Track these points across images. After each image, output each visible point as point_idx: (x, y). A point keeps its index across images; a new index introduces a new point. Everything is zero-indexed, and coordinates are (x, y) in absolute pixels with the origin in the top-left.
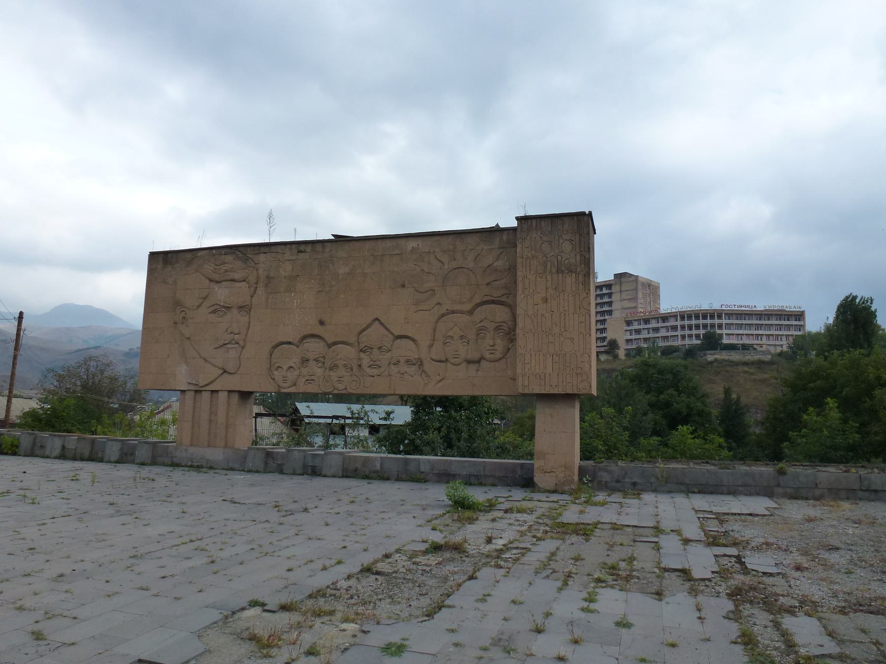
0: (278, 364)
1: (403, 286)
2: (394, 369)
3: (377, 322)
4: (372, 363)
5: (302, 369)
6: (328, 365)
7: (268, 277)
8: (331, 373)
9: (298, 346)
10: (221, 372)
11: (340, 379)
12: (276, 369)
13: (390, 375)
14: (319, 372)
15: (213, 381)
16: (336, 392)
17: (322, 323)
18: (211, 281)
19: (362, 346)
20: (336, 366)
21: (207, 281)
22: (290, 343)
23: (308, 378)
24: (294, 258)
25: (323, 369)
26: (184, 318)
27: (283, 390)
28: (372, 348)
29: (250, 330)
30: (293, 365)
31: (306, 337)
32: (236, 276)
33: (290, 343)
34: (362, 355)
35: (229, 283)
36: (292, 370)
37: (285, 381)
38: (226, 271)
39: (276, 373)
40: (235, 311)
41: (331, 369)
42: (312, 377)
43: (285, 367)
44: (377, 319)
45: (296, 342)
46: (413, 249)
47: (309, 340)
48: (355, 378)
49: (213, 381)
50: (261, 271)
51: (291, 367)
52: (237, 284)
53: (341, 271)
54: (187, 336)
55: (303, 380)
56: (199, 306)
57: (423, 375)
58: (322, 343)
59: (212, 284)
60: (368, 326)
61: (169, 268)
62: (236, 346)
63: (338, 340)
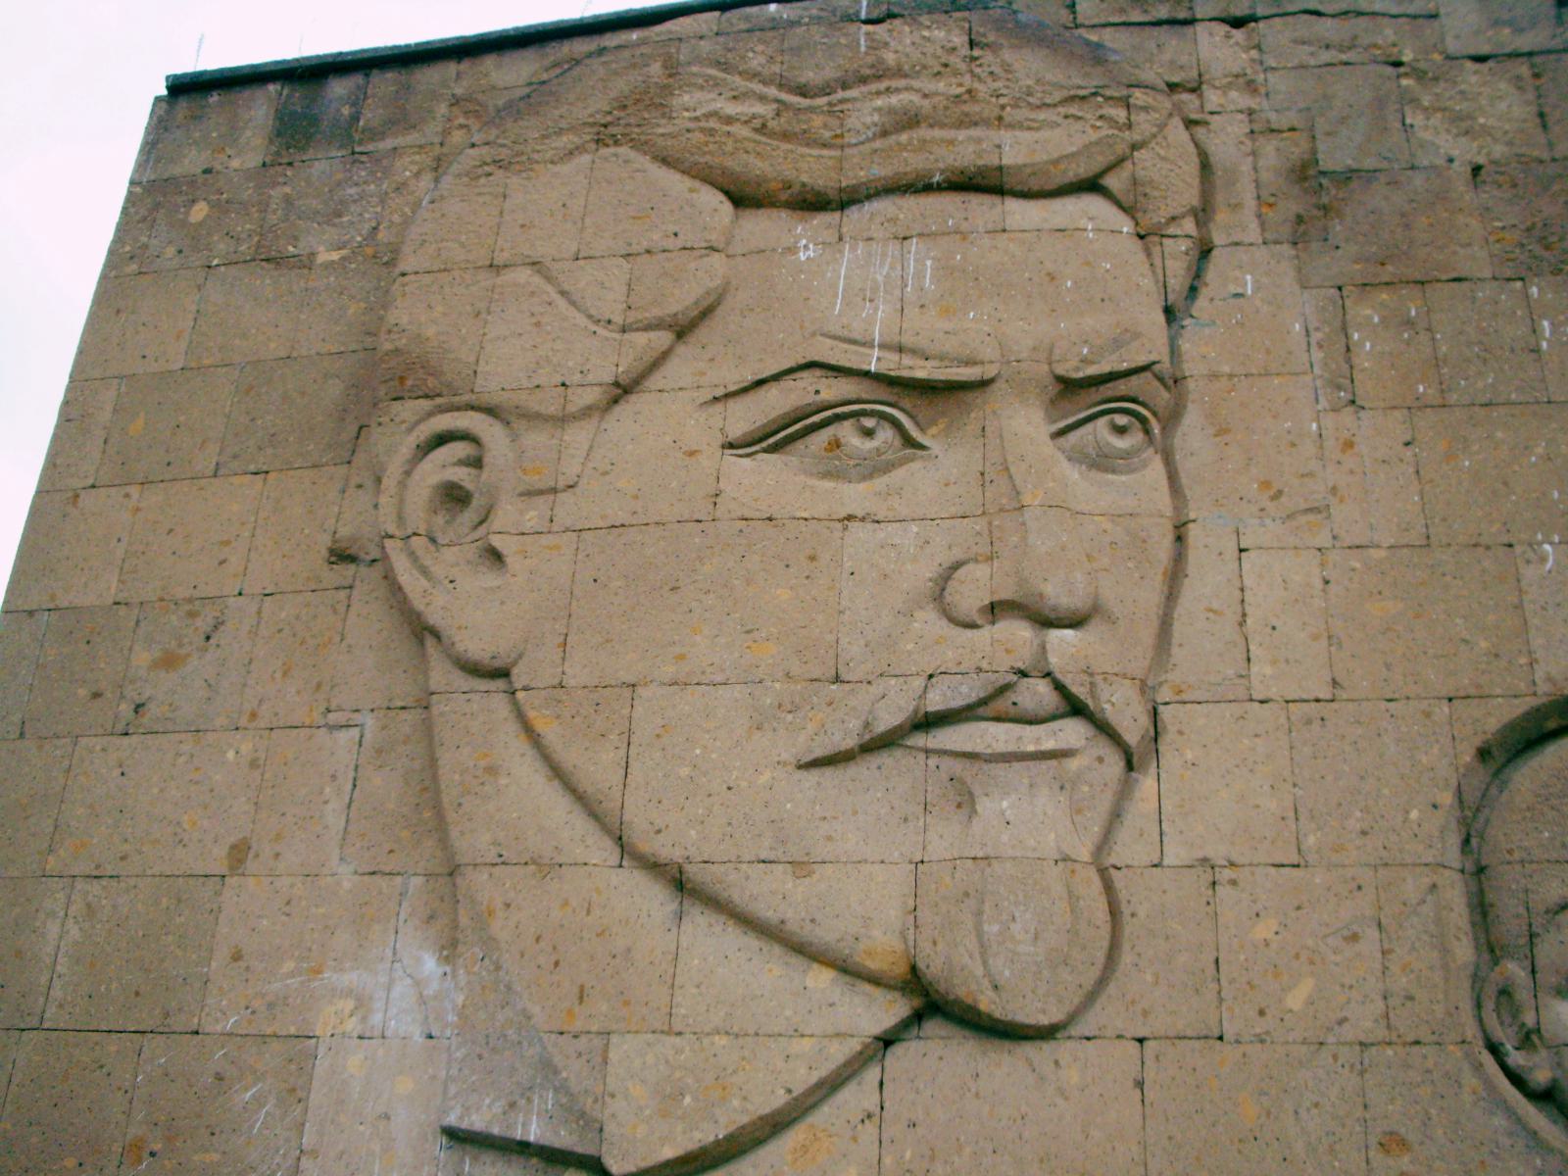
7: (1305, 173)
10: (886, 1011)
15: (774, 1125)
18: (742, 199)
21: (713, 201)
24: (1526, 42)
26: (454, 497)
29: (1206, 580)
32: (1014, 150)
35: (949, 205)
38: (910, 120)
40: (1025, 424)
49: (774, 1125)
50: (1226, 139)
52: (1020, 213)
54: (477, 646)
56: (622, 390)
59: (764, 227)
61: (322, 165)
62: (1072, 732)
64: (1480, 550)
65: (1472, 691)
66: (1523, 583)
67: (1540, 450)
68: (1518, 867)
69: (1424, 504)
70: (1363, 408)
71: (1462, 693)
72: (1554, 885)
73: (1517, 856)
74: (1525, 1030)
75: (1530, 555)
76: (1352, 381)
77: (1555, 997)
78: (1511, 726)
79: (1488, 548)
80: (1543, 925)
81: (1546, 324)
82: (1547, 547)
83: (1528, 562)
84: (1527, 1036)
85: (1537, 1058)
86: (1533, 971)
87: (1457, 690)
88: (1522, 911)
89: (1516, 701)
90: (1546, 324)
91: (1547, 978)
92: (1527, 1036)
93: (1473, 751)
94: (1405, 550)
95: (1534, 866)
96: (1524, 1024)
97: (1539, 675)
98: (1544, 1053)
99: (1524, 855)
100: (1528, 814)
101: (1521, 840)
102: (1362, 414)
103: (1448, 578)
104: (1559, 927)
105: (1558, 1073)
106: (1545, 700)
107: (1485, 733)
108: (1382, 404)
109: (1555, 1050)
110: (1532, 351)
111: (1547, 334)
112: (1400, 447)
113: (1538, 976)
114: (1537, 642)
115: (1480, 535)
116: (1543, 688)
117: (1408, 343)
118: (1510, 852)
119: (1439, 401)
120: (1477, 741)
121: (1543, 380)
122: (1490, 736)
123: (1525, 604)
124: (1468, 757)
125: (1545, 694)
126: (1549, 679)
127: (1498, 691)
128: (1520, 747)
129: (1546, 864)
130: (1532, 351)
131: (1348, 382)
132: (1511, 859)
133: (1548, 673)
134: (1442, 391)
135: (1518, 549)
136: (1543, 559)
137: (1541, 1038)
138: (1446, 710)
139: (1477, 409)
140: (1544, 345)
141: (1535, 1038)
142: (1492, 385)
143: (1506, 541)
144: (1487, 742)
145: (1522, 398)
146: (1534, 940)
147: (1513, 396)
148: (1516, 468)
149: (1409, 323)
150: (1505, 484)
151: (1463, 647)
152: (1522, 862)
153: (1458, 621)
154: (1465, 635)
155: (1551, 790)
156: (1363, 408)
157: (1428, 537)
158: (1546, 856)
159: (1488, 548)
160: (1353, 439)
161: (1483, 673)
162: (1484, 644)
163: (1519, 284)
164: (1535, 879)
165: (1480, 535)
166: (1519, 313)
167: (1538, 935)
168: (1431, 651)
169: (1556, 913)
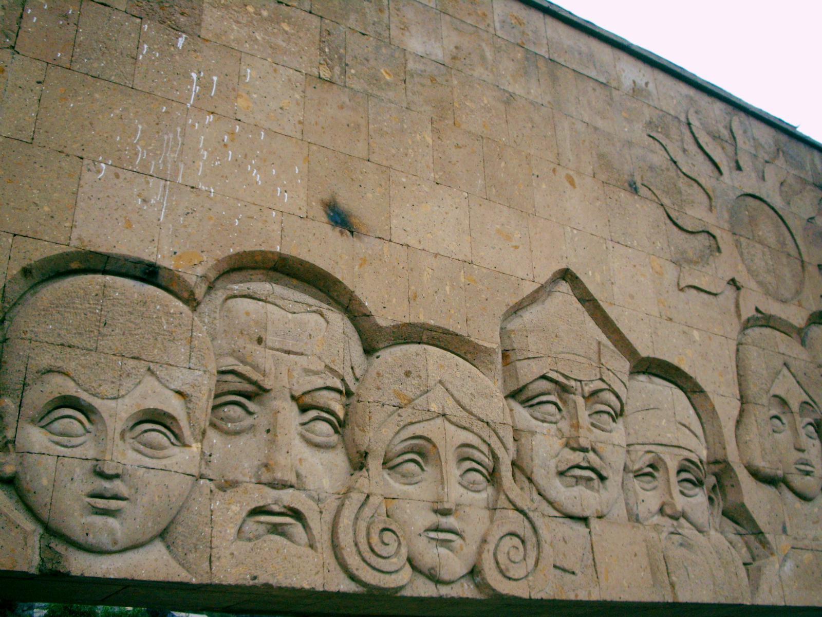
0: (70, 388)
1: (633, 188)
2: (649, 498)
3: (564, 287)
4: (577, 458)
5: (214, 437)
6: (380, 433)
8: (396, 486)
9: (192, 301)
11: (443, 521)
12: (43, 419)
13: (634, 518)
14: (321, 470)
16: (424, 589)
17: (340, 219)
19: (528, 371)
20: (422, 451)
22: (149, 273)
23: (269, 497)
25: (338, 459)
27: (80, 565)
28: (564, 389)
30: (174, 406)
31: (242, 266)
33: (149, 273)
34: (522, 415)
36: (157, 437)
37: (103, 502)
39: (35, 437)
41: (389, 464)
42: (288, 497)
43: (118, 411)
44: (566, 275)
45: (192, 276)
46: (637, 92)
47: (263, 287)
48: (514, 521)
51: (157, 418)
53: (415, 44)
55: (234, 508)
57: (729, 526)
58: (337, 319)
60: (533, 298)
63: (422, 317)
64: (63, 155)
65: (30, 234)
66: (82, 182)
67: (117, 112)
68: (27, 342)
69: (37, 119)
70: (18, 53)
71: (24, 233)
72: (46, 357)
73: (28, 336)
74: (6, 440)
75: (92, 168)
76: (17, 36)
77: (29, 423)
78: (48, 260)
79: (68, 155)
80: (33, 379)
81: (146, 46)
82: (103, 165)
83: (89, 170)
84: (6, 444)
85: (8, 459)
86: (20, 406)
87: (21, 231)
88: (22, 368)
89: (56, 246)
90: (146, 46)
91: (28, 411)
92: (6, 444)
93: (19, 269)
94: (15, 142)
95: (38, 344)
96: (5, 437)
97: (75, 235)
98: (13, 455)
99: (33, 336)
100: (43, 313)
101: (34, 327)
102: (16, 56)
103: (37, 166)
104: (43, 382)
105: (20, 469)
106: (73, 249)
107: (31, 260)
108: (31, 55)
109: (21, 454)
110: (133, 58)
111: (144, 52)
112: (34, 83)
113: (22, 409)
114: (80, 216)
115: (65, 147)
116: (75, 243)
117: (61, 27)
118: (25, 332)
119: (68, 66)
120: (25, 263)
121: (133, 75)
122: (33, 262)
123: (79, 193)
124: (15, 271)
125: (74, 247)
126: (79, 239)
127: (47, 238)
128: (52, 274)
129: (45, 344)
130: (133, 58)
131: (15, 35)
132: (24, 337)
133: (80, 235)
134: (71, 61)
135: (86, 162)
136: (99, 172)
137: (14, 445)
138: (10, 240)
139: (89, 78)
140: (141, 57)
141: (10, 446)
142: (103, 68)
143: (80, 155)
144: (31, 265)
145: (117, 81)
146: (25, 388)
147: (113, 78)
148: (100, 117)
149: (66, 17)
150: (91, 124)
151: (33, 207)
152: (30, 340)
153: (35, 191)
154: (37, 201)
155: (61, 302)
156: (18, 53)
157: (33, 139)
158: (46, 339)
159: (68, 155)
160: (5, 68)
161: (40, 225)
162: (46, 209)
163: (138, 21)
164: (36, 351)
165: (65, 147)
166: (133, 35)
167: (29, 385)
168: (12, 204)
169: (44, 373)
